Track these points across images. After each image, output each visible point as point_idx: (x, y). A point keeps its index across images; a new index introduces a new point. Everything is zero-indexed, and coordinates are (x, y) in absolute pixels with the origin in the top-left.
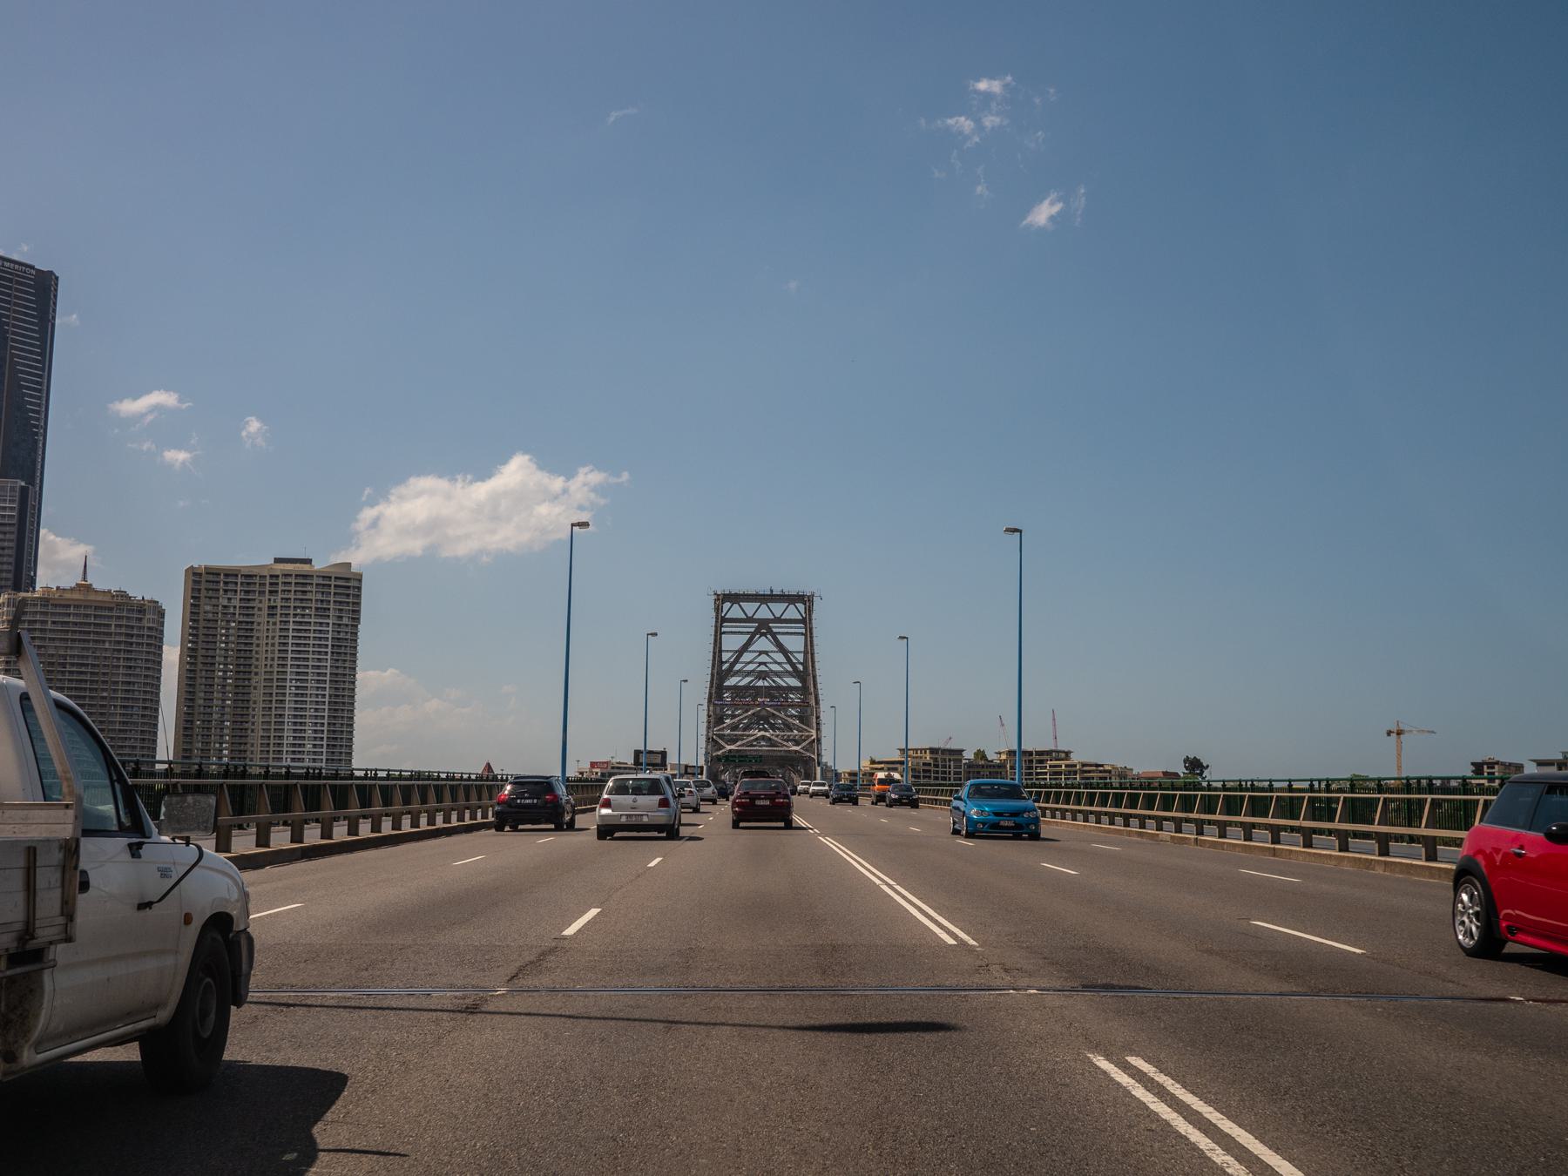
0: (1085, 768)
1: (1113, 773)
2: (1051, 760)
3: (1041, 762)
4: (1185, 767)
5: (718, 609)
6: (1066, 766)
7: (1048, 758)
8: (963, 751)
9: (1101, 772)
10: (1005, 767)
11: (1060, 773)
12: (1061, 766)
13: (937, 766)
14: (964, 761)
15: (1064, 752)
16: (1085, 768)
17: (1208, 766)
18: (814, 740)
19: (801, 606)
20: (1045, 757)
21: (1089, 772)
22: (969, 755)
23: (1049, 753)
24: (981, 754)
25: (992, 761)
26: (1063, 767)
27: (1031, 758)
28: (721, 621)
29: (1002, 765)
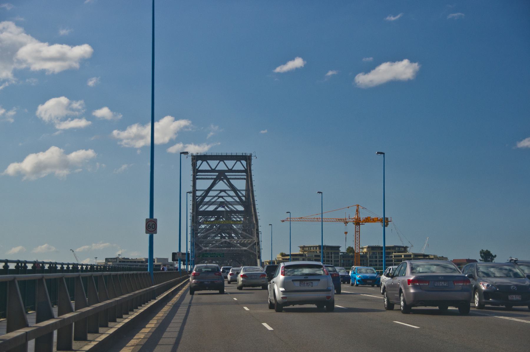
2: (395, 252)
3: (389, 253)
4: (481, 256)
5: (194, 165)
6: (405, 256)
7: (393, 251)
8: (339, 247)
10: (366, 257)
12: (401, 256)
14: (340, 254)
15: (403, 247)
17: (495, 256)
18: (255, 244)
19: (244, 162)
22: (343, 250)
23: (394, 248)
26: (403, 257)
28: (196, 171)
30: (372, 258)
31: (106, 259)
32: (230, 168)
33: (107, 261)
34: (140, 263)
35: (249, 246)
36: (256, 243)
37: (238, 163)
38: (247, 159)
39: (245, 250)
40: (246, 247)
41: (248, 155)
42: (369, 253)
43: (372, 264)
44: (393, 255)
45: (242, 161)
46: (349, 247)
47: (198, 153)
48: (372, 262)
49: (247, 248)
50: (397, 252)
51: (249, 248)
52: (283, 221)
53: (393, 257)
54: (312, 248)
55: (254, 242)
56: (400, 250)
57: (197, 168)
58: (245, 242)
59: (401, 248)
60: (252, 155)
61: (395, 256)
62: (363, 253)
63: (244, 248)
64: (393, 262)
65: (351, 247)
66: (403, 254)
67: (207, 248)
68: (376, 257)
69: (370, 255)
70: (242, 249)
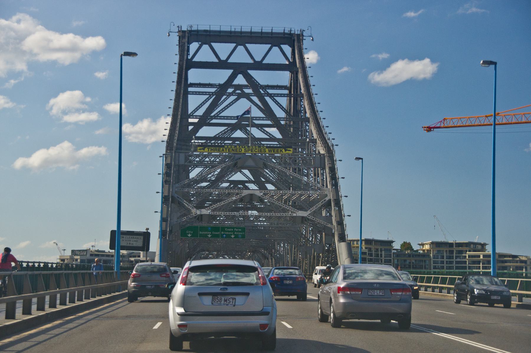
0: (502, 259)
1: (528, 263)
2: (470, 251)
3: (461, 252)
5: (183, 49)
6: (484, 256)
7: (468, 249)
8: (392, 242)
9: (517, 262)
10: (429, 256)
11: (479, 262)
12: (479, 256)
13: (371, 255)
14: (393, 251)
15: (480, 244)
16: (502, 259)
18: (329, 203)
19: (287, 49)
20: (464, 248)
21: (506, 262)
22: (397, 246)
23: (468, 244)
24: (407, 246)
25: (417, 251)
26: (481, 257)
27: (451, 249)
29: (426, 255)
30: (436, 259)
31: (73, 251)
32: (258, 59)
33: (73, 254)
34: (104, 256)
35: (314, 208)
36: (330, 200)
37: (276, 49)
38: (294, 40)
39: (303, 217)
40: (306, 211)
41: (296, 33)
42: (433, 251)
43: (437, 267)
44: (467, 255)
45: (283, 46)
46: (404, 242)
47: (191, 27)
48: (436, 264)
49: (309, 212)
50: (472, 250)
51: (314, 214)
52: (429, 129)
53: (467, 258)
54: (356, 242)
55: (327, 199)
56: (476, 247)
57: (189, 57)
58: (303, 198)
59: (477, 246)
60: (304, 34)
61: (469, 256)
62: (424, 251)
63: (300, 212)
64: (466, 264)
65: (408, 242)
66: (481, 254)
67: (203, 210)
68: (443, 257)
69: (434, 253)
70: (295, 215)
